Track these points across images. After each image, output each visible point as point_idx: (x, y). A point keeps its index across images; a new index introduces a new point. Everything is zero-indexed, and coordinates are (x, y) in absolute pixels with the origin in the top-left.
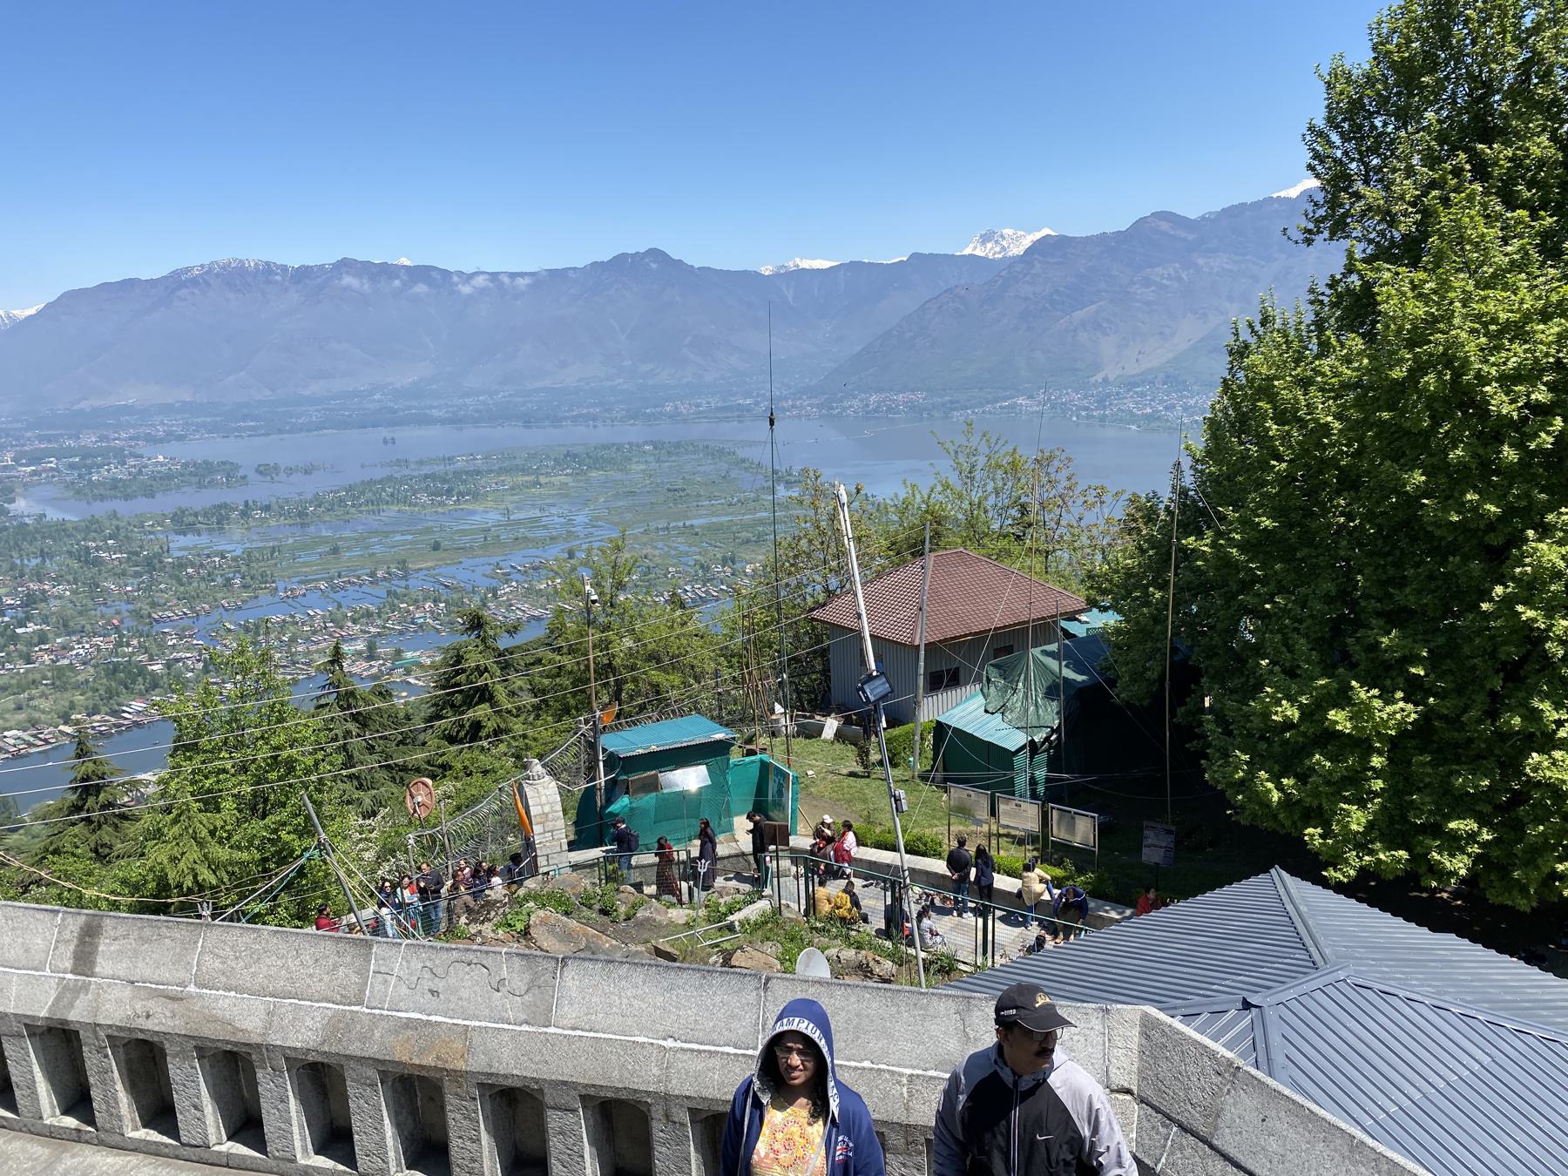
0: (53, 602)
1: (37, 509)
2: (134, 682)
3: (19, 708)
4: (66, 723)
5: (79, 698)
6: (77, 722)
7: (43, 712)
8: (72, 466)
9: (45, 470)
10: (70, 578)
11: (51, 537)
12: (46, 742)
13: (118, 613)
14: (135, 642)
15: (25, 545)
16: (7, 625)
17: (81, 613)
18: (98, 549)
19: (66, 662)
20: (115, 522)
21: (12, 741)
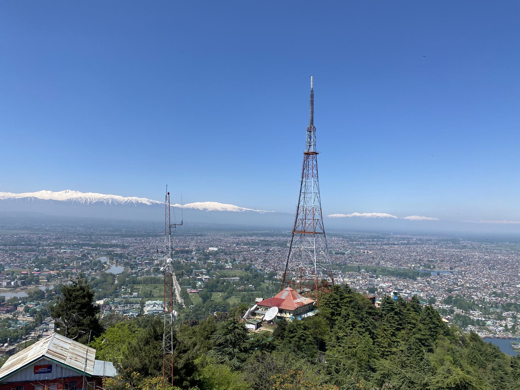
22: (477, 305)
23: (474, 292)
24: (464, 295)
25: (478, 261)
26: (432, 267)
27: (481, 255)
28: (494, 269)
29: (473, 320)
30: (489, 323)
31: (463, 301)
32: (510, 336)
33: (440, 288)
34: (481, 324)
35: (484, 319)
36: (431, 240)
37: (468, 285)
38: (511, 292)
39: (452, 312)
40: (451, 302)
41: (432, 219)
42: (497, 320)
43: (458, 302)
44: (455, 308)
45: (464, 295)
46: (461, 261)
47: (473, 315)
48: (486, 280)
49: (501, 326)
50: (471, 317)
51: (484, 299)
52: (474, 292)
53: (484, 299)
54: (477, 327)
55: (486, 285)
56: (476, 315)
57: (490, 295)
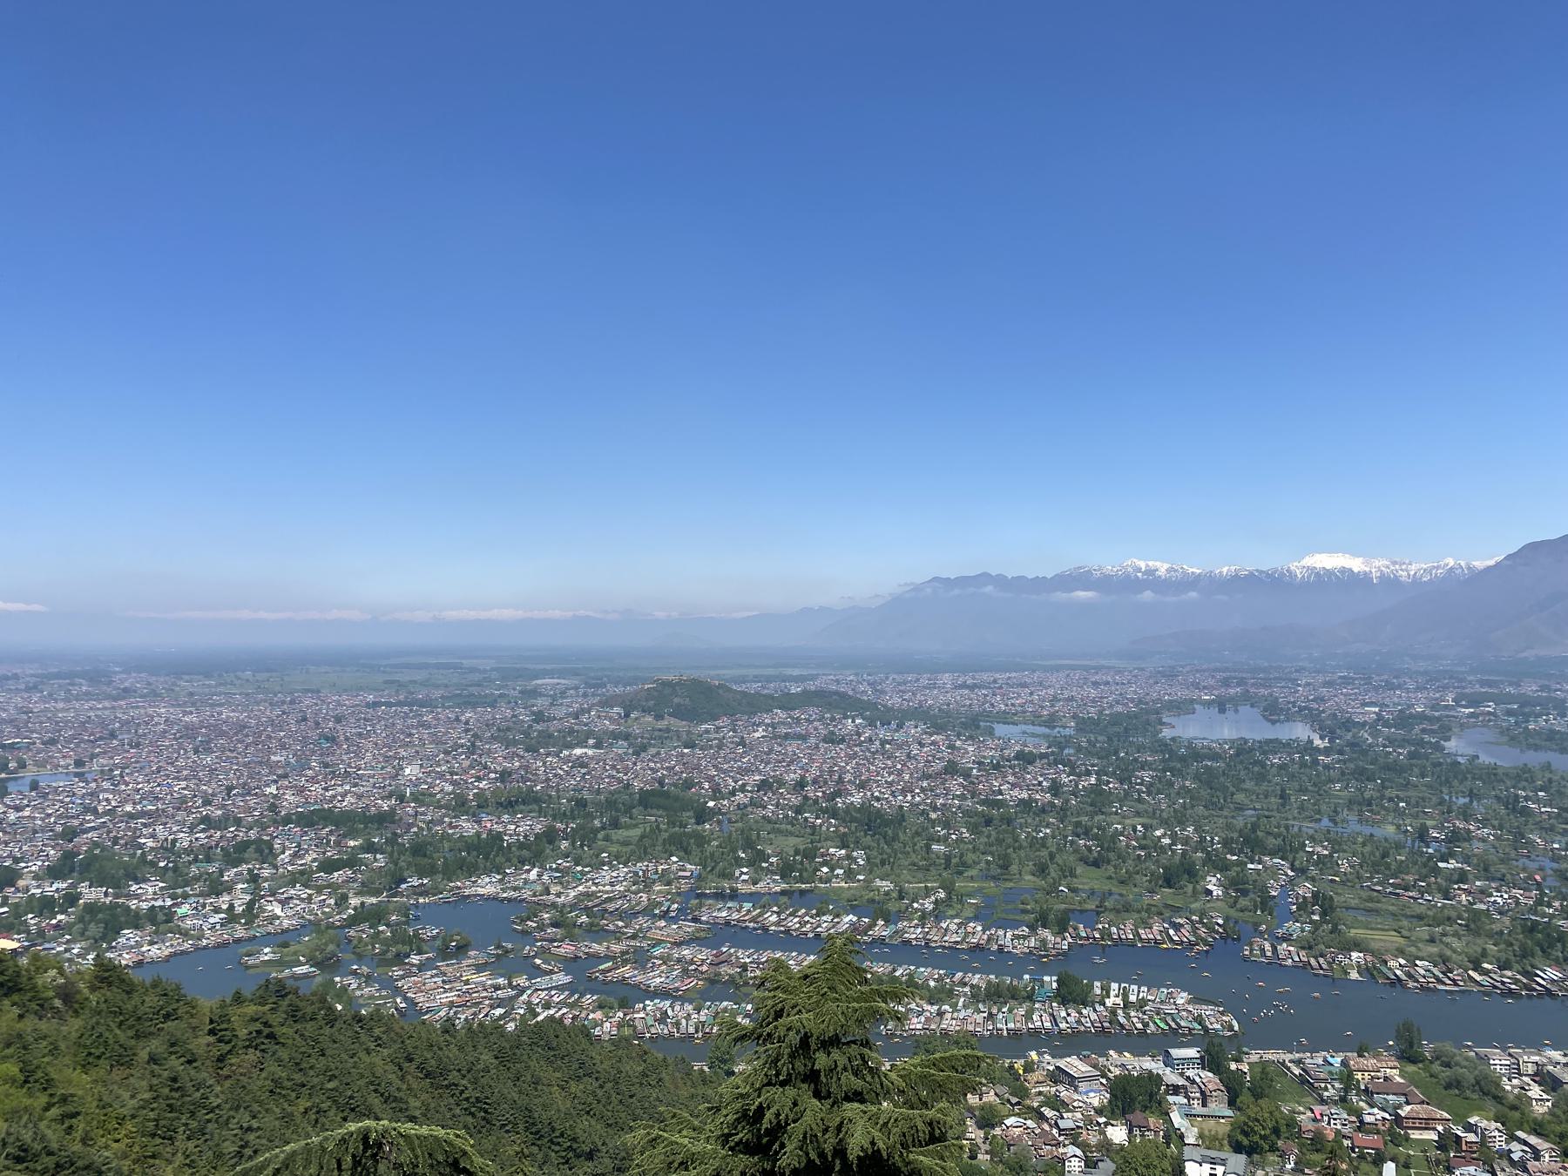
0: (1476, 844)
1: (1470, 751)
2: (1551, 946)
3: (1432, 941)
4: (1475, 970)
5: (1491, 947)
6: (1486, 973)
7: (1454, 951)
8: (1509, 713)
9: (1483, 714)
10: (1496, 823)
11: (1480, 779)
12: (1455, 983)
13: (1541, 869)
14: (1557, 904)
15: (1456, 783)
16: (1431, 857)
17: (1502, 861)
18: (1527, 799)
19: (1484, 907)
20: (1548, 775)
21: (1422, 972)
22: (153, 864)
23: (145, 825)
24: (115, 841)
25: (165, 731)
26: (12, 765)
27: (175, 713)
28: (209, 751)
29: (137, 913)
30: (184, 910)
31: (111, 859)
32: (240, 932)
33: (35, 832)
34: (161, 917)
35: (169, 902)
36: (16, 677)
37: (129, 808)
38: (249, 810)
39: (72, 899)
40: (72, 870)
41: (21, 606)
42: (209, 895)
43: (95, 867)
44: (83, 888)
45: (115, 842)
46: (113, 735)
47: (137, 897)
48: (183, 784)
49: (217, 910)
50: (133, 904)
51: (174, 841)
52: (145, 825)
53: (174, 841)
54: (150, 928)
55: (183, 800)
56: (147, 894)
57: (192, 829)
